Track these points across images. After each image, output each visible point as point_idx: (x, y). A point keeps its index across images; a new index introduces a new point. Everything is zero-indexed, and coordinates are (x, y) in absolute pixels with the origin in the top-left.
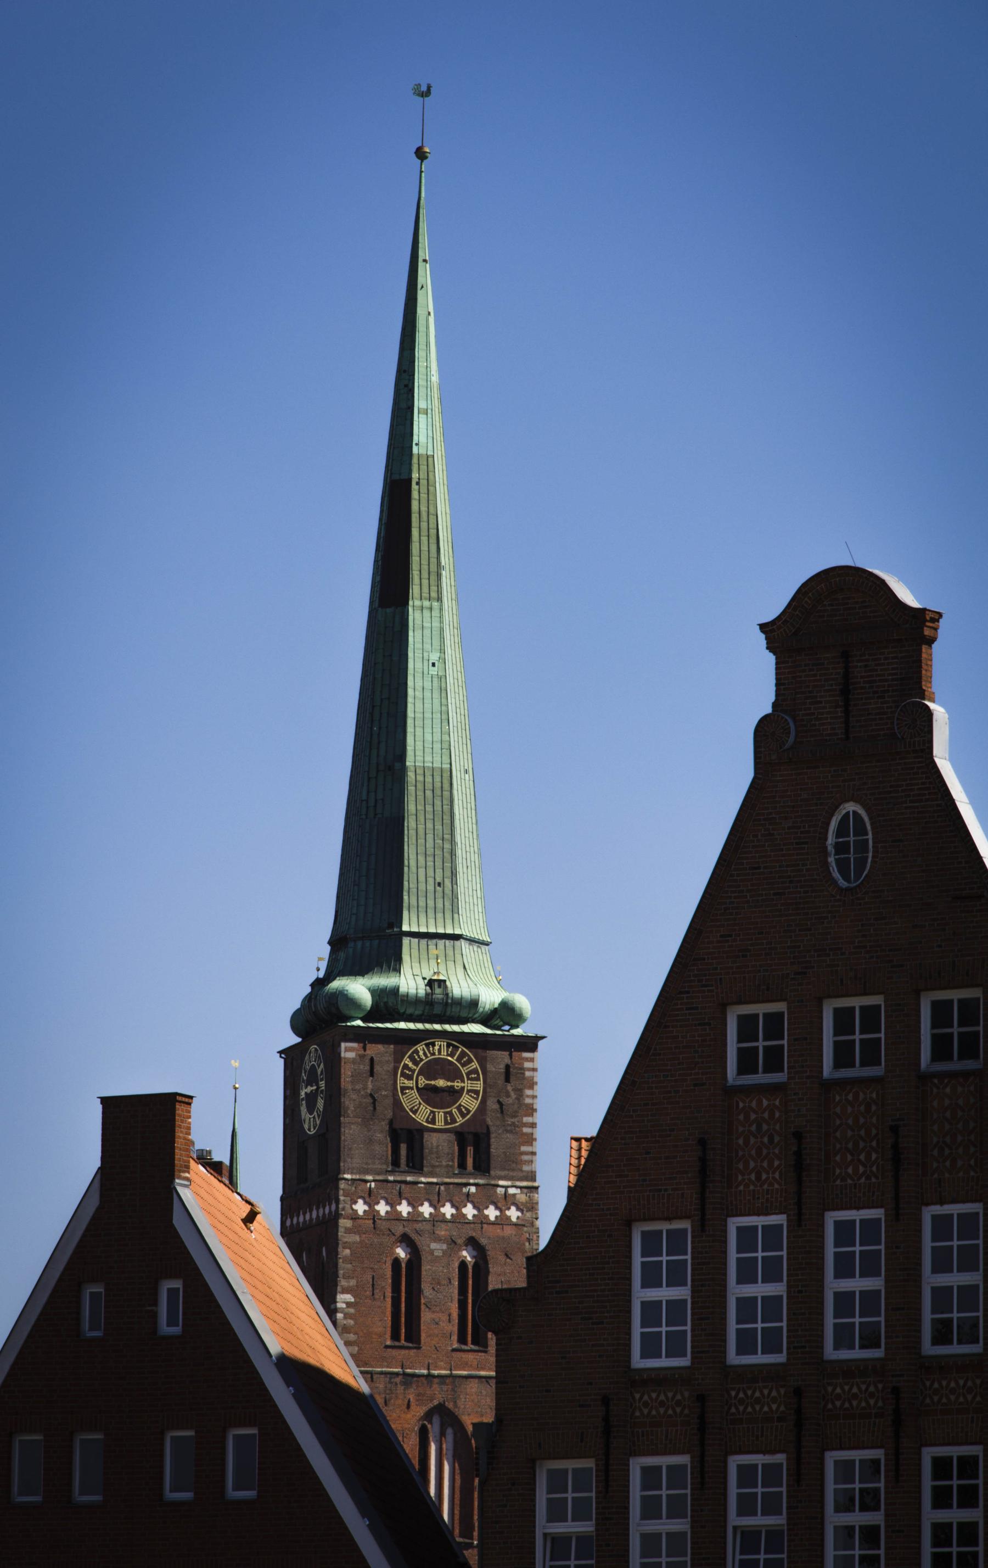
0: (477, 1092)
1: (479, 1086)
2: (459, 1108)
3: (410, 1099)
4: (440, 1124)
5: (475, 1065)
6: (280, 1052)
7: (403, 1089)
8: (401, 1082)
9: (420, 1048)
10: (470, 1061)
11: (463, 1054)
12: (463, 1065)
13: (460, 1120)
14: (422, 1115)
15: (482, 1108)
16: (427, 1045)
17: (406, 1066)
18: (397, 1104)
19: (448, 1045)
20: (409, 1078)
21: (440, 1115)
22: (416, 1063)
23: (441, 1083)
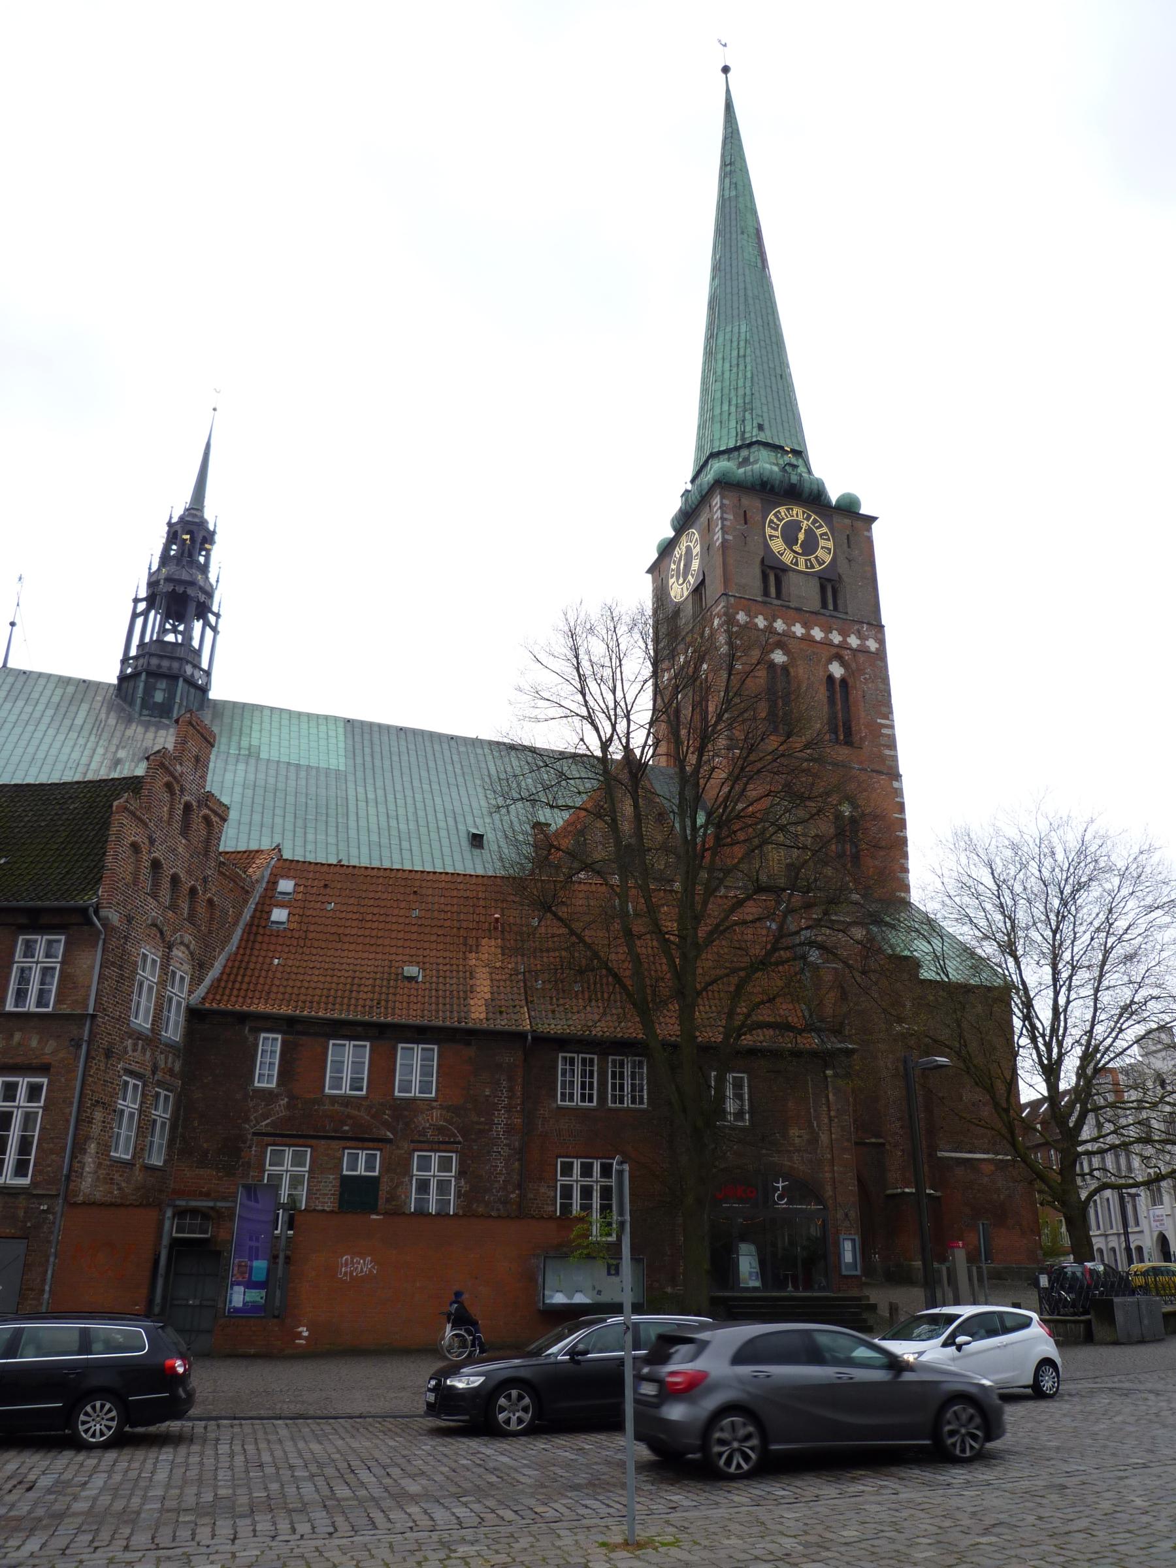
0: (829, 549)
1: (830, 544)
2: (816, 558)
3: (777, 545)
4: (802, 567)
5: (825, 529)
6: (648, 572)
7: (771, 536)
8: (768, 531)
9: (782, 510)
10: (820, 526)
11: (815, 521)
12: (818, 528)
13: (818, 568)
14: (788, 558)
15: (834, 560)
16: (788, 510)
17: (771, 521)
18: (767, 546)
19: (804, 513)
20: (776, 530)
21: (802, 560)
22: (780, 520)
23: (801, 536)
